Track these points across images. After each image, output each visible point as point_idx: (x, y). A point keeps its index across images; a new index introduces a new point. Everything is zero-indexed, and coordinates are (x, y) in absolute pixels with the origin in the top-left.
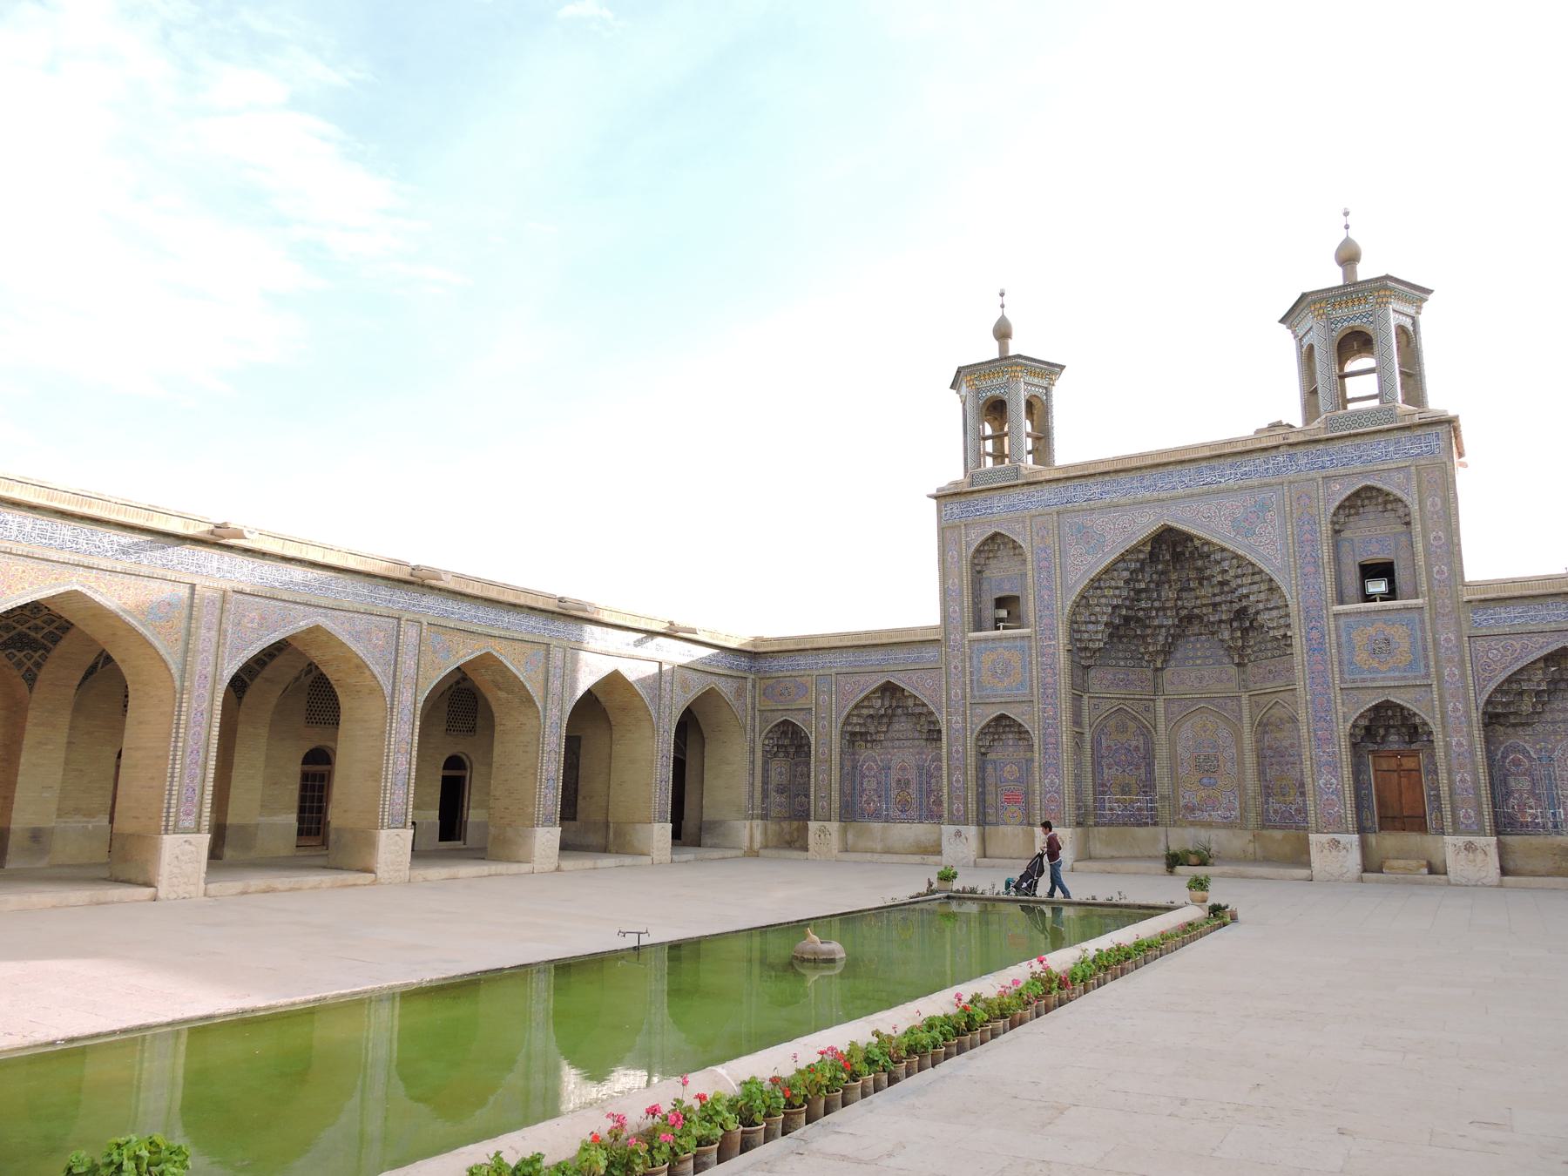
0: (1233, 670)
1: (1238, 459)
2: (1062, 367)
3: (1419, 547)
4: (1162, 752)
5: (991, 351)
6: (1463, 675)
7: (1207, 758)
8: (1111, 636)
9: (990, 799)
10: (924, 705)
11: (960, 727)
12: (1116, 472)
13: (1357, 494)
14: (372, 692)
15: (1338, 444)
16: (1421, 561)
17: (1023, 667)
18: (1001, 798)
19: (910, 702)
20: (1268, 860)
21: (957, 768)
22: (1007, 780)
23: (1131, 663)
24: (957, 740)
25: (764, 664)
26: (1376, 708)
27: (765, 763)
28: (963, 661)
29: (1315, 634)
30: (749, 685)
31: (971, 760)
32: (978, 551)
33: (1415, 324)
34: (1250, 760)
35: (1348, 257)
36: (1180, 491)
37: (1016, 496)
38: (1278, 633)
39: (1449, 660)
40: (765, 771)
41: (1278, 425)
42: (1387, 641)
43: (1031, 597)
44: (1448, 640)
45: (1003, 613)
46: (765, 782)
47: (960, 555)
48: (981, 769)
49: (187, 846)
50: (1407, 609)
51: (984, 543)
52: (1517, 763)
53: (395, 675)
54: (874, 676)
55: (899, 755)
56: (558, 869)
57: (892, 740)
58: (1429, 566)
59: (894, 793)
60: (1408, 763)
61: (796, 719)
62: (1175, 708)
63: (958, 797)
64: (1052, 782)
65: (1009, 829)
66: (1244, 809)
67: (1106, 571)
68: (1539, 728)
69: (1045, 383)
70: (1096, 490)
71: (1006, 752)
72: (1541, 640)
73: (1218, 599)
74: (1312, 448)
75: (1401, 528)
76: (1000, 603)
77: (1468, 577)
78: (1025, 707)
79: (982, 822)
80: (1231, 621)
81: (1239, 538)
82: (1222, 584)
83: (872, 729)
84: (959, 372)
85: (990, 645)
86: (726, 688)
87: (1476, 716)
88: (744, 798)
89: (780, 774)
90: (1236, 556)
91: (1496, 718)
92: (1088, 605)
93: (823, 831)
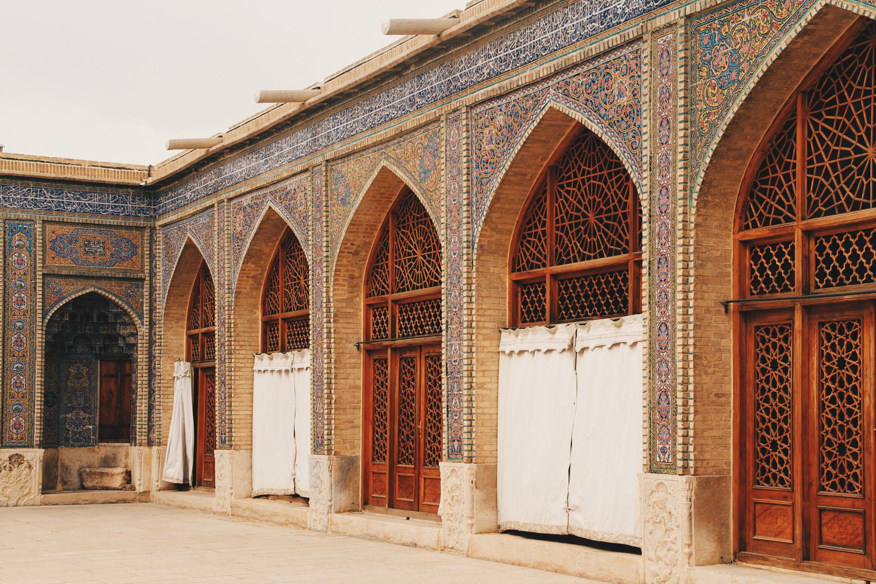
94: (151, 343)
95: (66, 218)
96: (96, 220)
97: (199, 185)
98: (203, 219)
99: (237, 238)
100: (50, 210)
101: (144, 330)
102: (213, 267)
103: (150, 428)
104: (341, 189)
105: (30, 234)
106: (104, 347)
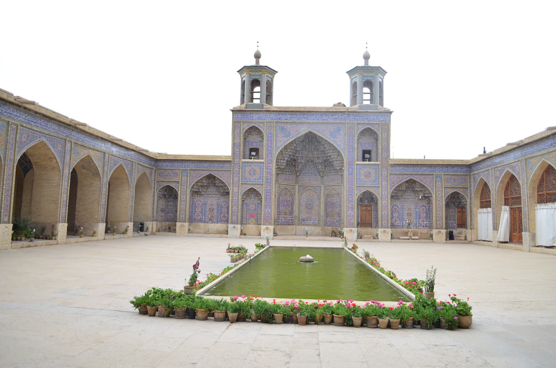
0: (320, 178)
1: (334, 114)
2: (277, 72)
3: (380, 147)
4: (296, 202)
5: (252, 62)
6: (387, 185)
7: (310, 204)
8: (287, 165)
9: (244, 216)
10: (223, 183)
11: (236, 191)
12: (296, 111)
13: (364, 129)
14: (53, 168)
15: (362, 114)
16: (380, 151)
17: (260, 172)
18: (248, 215)
19: (217, 182)
20: (326, 235)
21: (235, 205)
22: (250, 210)
23: (290, 173)
24: (235, 195)
25: (160, 164)
26: (364, 193)
27: (158, 201)
28: (239, 169)
29: (350, 170)
30: (154, 171)
31: (240, 203)
32: (246, 131)
33: (382, 80)
34: (322, 206)
35: (367, 57)
36: (315, 121)
37: (262, 115)
38: (338, 168)
39: (384, 180)
40: (157, 203)
41: (339, 103)
42: (369, 173)
43: (265, 149)
44: (384, 174)
45: (254, 153)
46: (157, 208)
47: (240, 131)
48: (242, 206)
49: (6, 229)
50: (375, 165)
51: (249, 129)
52: (395, 209)
53: (64, 162)
54: (205, 172)
55: (212, 200)
56: (104, 239)
57: (208, 194)
58: (382, 153)
59: (207, 213)
60: (369, 208)
61: (173, 185)
62: (301, 188)
63: (235, 215)
64: (268, 211)
65: (251, 226)
66: (319, 221)
67: (289, 144)
68: (401, 200)
69: (271, 77)
70: (289, 116)
71: (252, 201)
72: (406, 176)
73: (319, 156)
74: (355, 114)
75: (375, 141)
76: (252, 150)
77: (391, 157)
78: (260, 186)
79: (242, 224)
80: (322, 163)
81: (332, 138)
82: (322, 151)
83: (201, 190)
84: (244, 67)
85: (249, 164)
87: (389, 196)
88: (150, 214)
89: (163, 205)
90: (329, 143)
91: (394, 197)
92: (282, 154)
93: (182, 226)
94: (471, 203)
95: (449, 173)
96: (456, 174)
97: (484, 164)
98: (485, 173)
99: (498, 178)
100: (445, 172)
101: (468, 200)
102: (490, 185)
103: (471, 225)
104: (530, 166)
105: (441, 178)
106: (458, 205)
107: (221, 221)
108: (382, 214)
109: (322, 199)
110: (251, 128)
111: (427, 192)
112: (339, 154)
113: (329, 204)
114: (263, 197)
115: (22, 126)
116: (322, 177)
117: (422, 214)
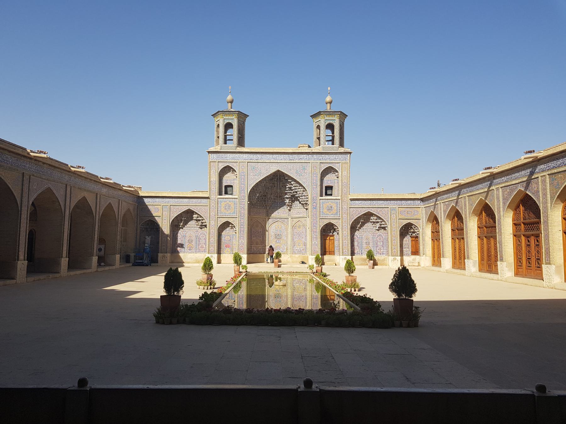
3: (340, 184)
26: (326, 225)
29: (314, 204)
34: (289, 236)
65: (226, 255)
66: (287, 249)
76: (226, 187)
80: (289, 198)
86: (131, 209)
87: (349, 227)
90: (295, 181)
91: (354, 228)
93: (164, 256)
107: (199, 251)
108: (343, 243)
109: (290, 230)
110: (225, 167)
111: (383, 223)
112: (305, 190)
113: (295, 234)
114: (237, 229)
115: (34, 175)
116: (290, 210)
117: (379, 243)
